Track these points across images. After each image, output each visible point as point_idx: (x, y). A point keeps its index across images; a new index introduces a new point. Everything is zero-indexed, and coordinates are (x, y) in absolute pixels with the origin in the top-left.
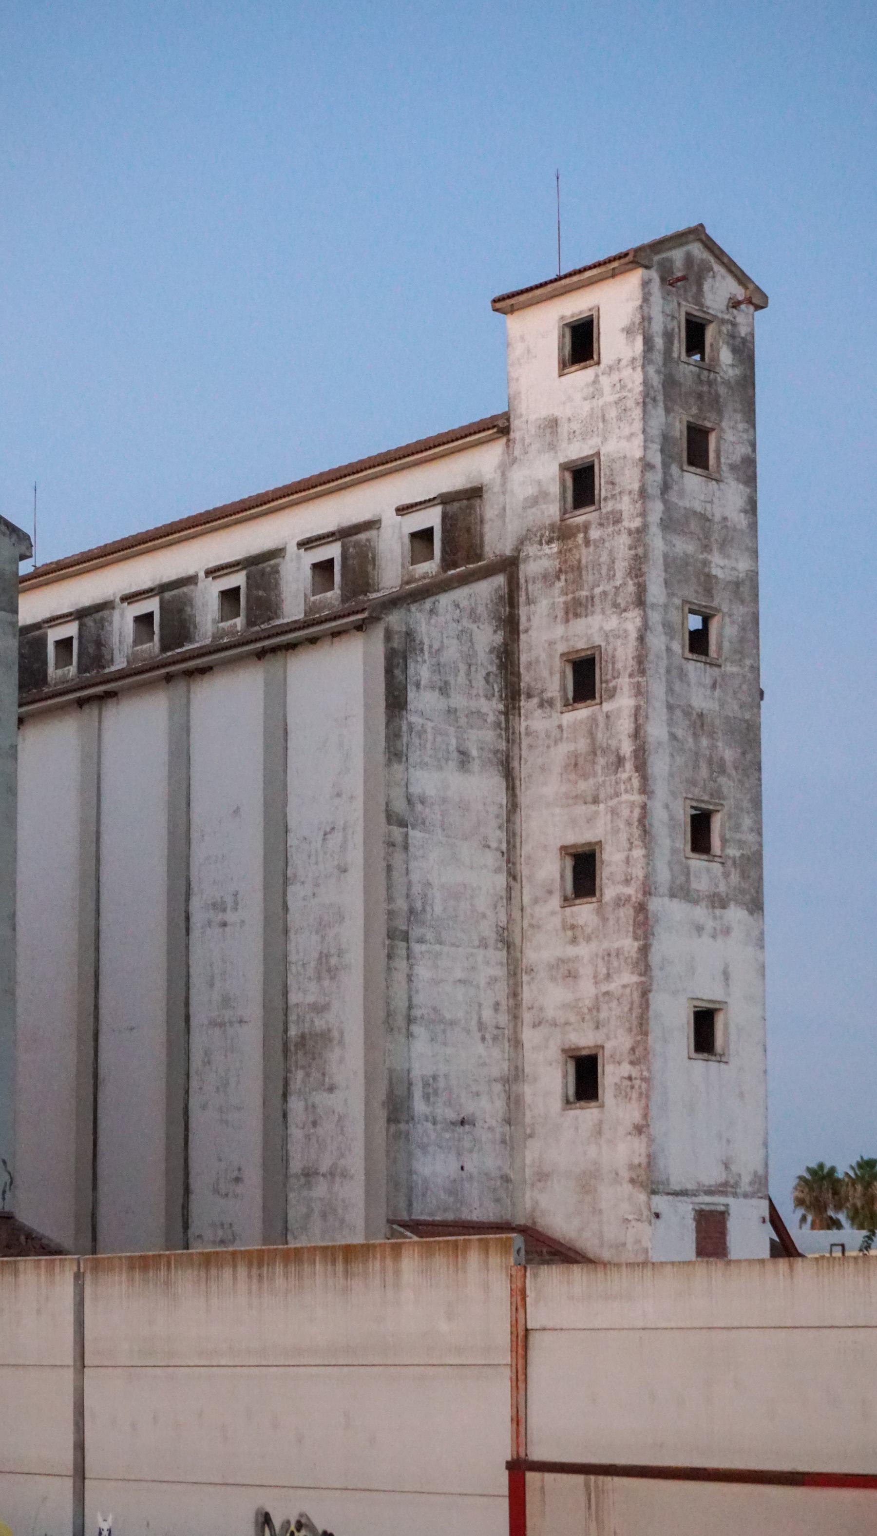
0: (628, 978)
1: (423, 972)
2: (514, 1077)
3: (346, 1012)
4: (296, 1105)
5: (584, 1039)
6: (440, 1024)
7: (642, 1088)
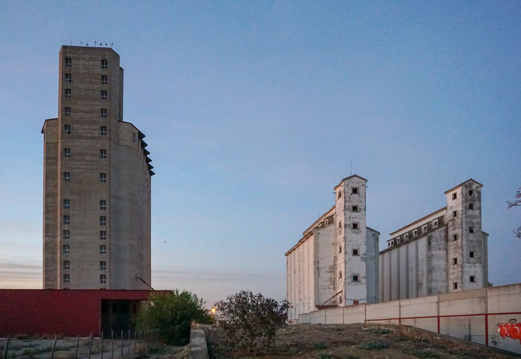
0: (460, 274)
1: (434, 275)
2: (447, 286)
3: (424, 281)
4: (419, 291)
5: (455, 281)
6: (436, 281)
7: (462, 287)
